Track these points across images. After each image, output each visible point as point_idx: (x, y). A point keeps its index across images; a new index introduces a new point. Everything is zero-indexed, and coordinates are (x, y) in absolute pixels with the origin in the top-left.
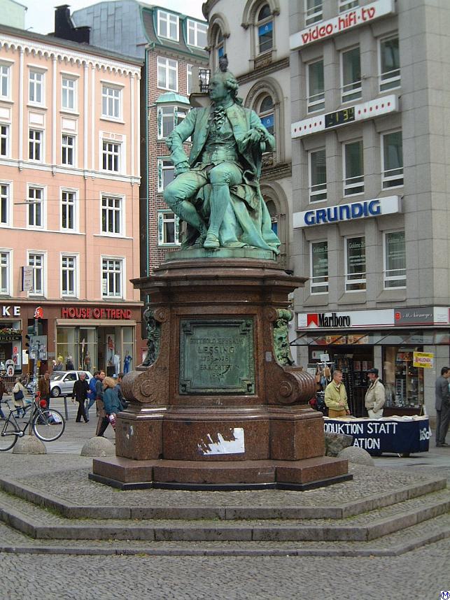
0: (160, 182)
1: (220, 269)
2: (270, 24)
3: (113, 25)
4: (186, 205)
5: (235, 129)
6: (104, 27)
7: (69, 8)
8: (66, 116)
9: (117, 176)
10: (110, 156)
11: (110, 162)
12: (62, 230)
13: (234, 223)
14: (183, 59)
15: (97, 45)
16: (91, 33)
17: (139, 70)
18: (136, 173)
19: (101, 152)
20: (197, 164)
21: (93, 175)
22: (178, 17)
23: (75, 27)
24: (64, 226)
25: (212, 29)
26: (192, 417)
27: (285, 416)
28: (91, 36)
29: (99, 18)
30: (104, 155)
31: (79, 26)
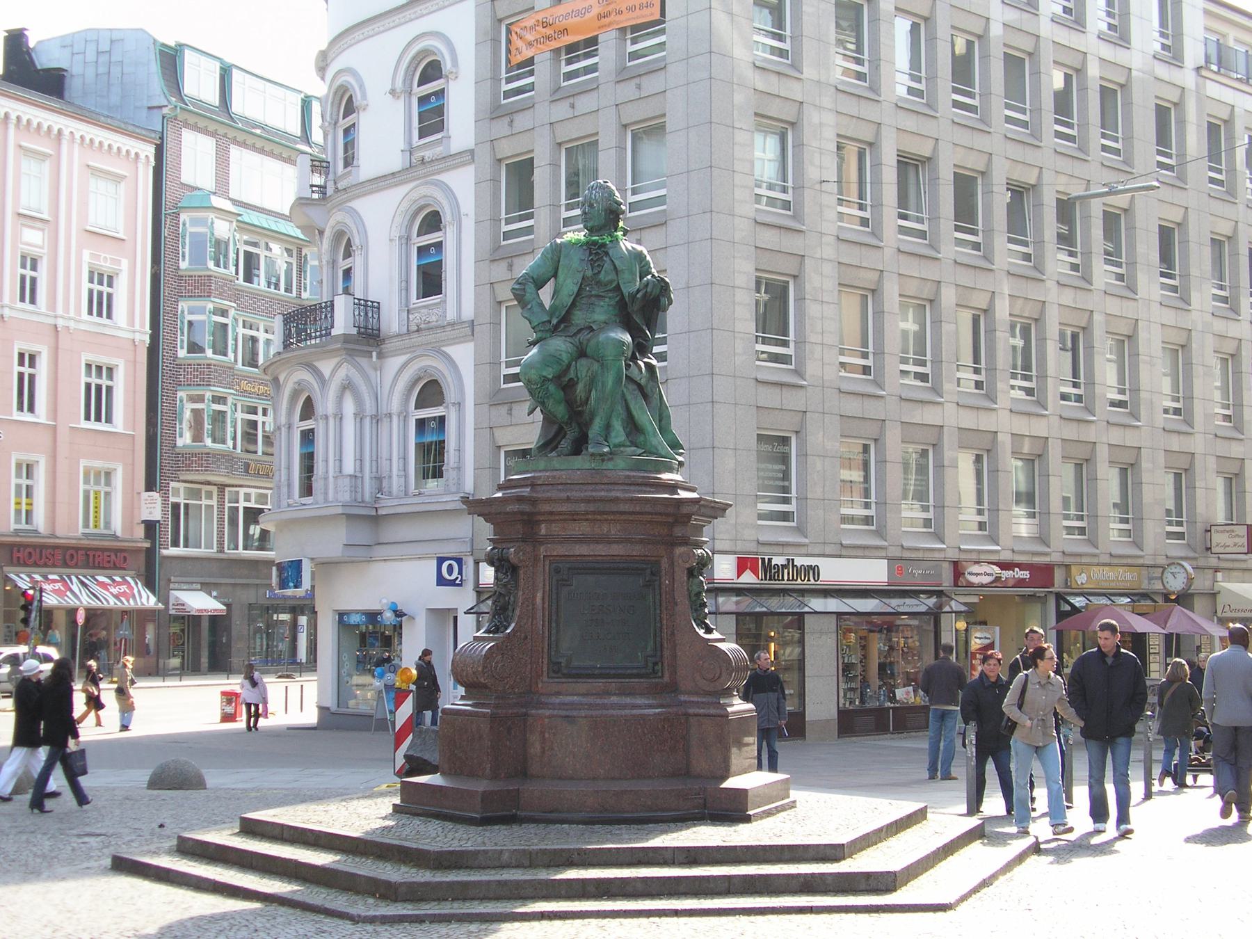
0: (182, 341)
1: (616, 487)
2: (440, 94)
3: (107, 70)
4: (552, 388)
6: (90, 72)
7: (26, 32)
8: (26, 222)
9: (110, 327)
10: (100, 294)
11: (101, 305)
12: (17, 416)
13: (624, 415)
14: (225, 135)
15: (78, 102)
16: (67, 81)
17: (150, 150)
18: (143, 325)
19: (86, 285)
20: (562, 326)
21: (72, 324)
22: (218, 65)
23: (39, 67)
24: (21, 408)
25: (335, 93)
28: (66, 86)
29: (81, 56)
30: (91, 292)
31: (45, 67)
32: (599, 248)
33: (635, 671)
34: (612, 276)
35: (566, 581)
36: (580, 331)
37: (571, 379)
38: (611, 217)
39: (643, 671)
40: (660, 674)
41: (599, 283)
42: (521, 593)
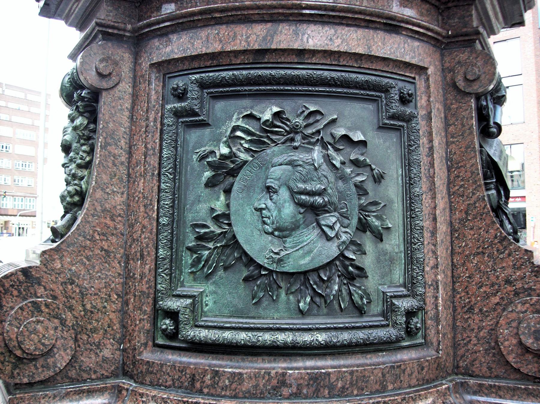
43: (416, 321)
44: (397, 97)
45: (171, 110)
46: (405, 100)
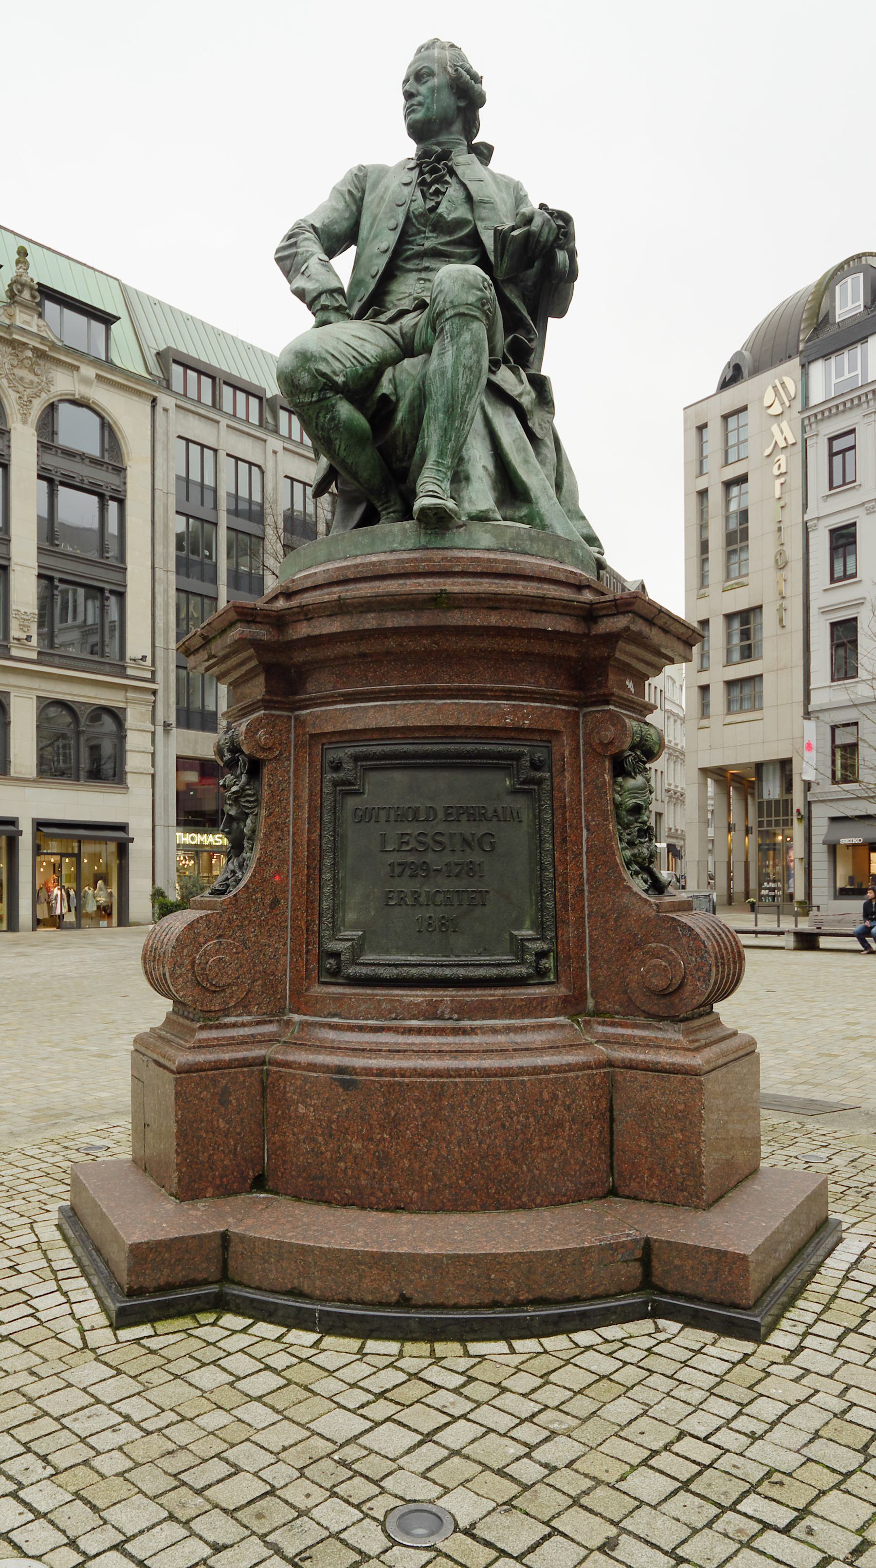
5: (483, 212)
26: (359, 1062)
27: (664, 1058)
32: (438, 160)
33: (494, 972)
34: (462, 212)
35: (351, 784)
36: (402, 313)
37: (384, 396)
38: (462, 104)
39: (513, 971)
40: (552, 977)
41: (440, 226)
42: (264, 813)
43: (548, 963)
44: (528, 764)
45: (330, 781)
46: (536, 766)
